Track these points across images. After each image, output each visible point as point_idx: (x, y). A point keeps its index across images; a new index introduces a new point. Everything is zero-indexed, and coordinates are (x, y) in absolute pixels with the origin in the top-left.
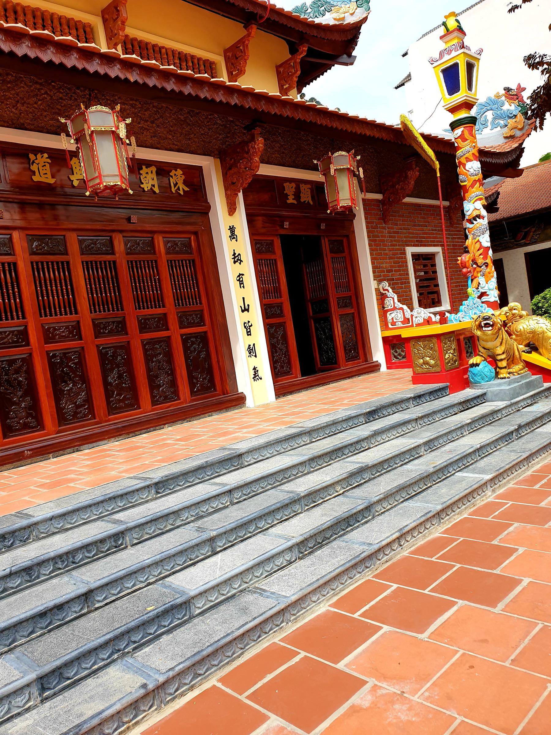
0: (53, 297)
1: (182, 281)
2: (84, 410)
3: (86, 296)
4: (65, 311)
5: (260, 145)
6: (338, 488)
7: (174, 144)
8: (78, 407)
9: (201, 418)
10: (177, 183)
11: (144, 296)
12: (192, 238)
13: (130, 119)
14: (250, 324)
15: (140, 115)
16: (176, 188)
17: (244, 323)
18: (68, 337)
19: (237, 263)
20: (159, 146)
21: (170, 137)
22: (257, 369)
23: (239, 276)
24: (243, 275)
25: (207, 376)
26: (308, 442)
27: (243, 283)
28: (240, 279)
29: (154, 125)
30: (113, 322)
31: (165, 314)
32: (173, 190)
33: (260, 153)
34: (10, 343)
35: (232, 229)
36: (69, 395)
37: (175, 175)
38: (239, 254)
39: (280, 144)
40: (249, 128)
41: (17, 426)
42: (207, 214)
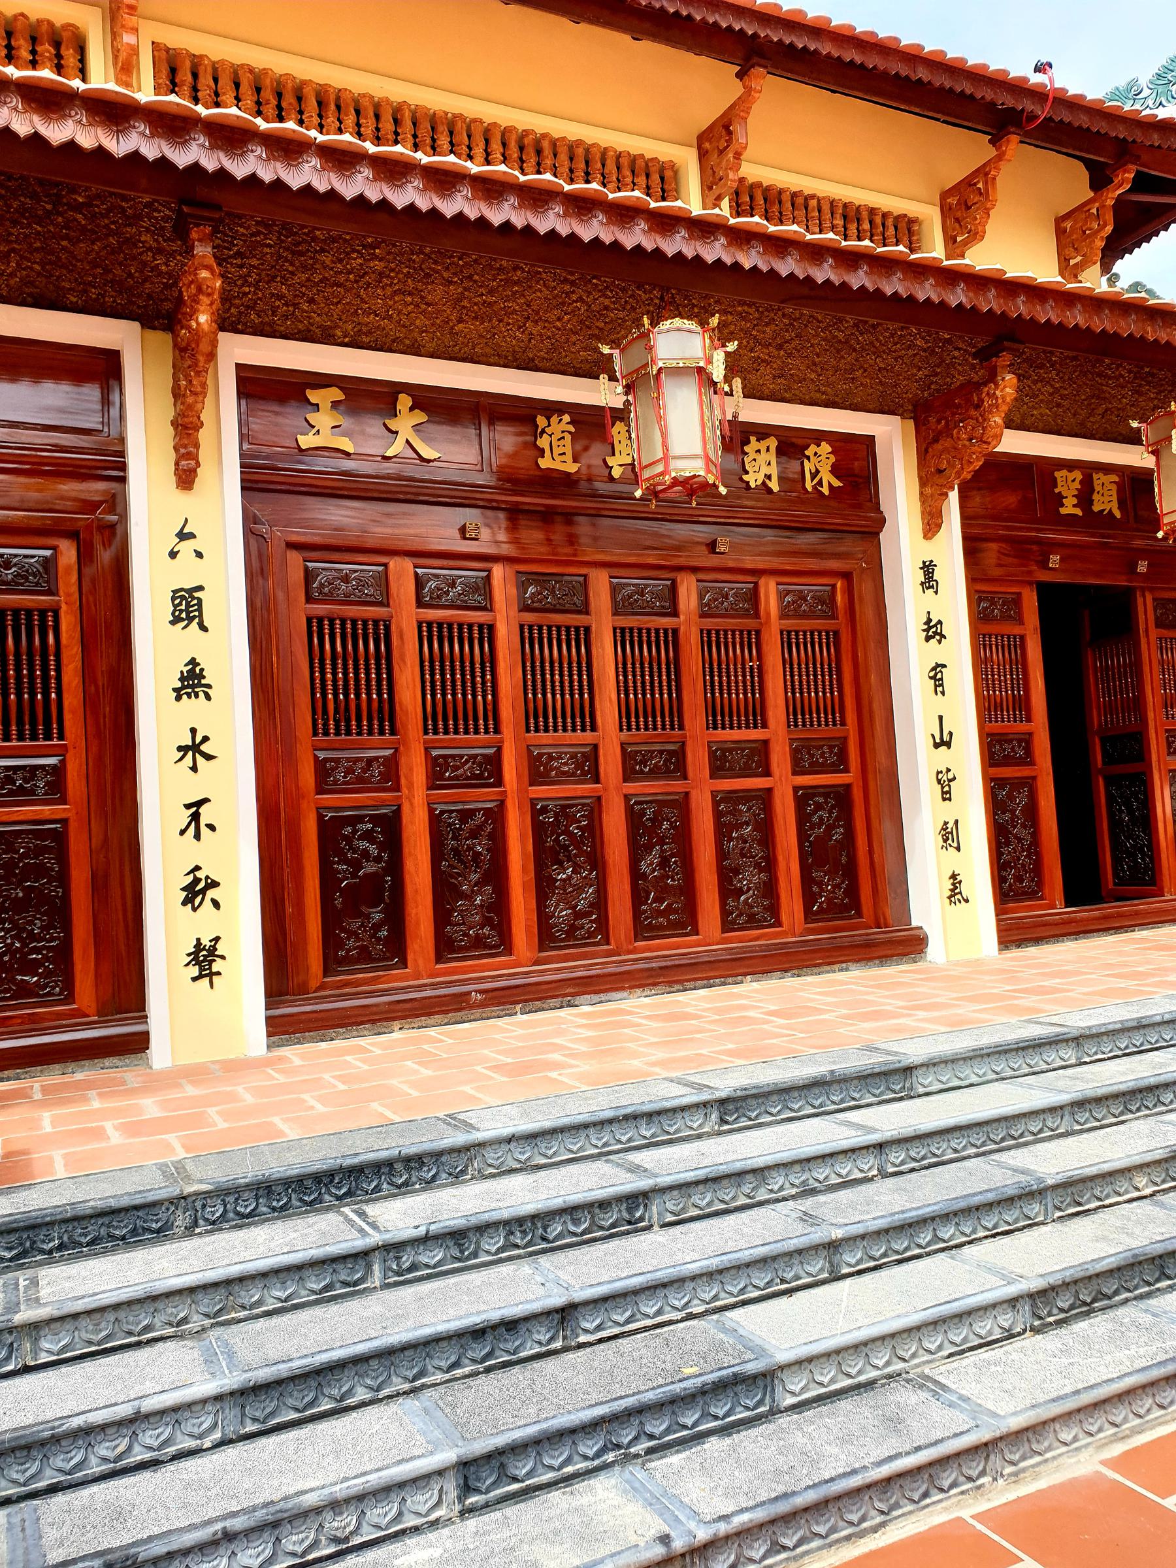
0: (554, 695)
1: (808, 676)
2: (588, 924)
3: (614, 697)
5: (1008, 390)
6: (1141, 1181)
7: (819, 391)
8: (578, 915)
9: (822, 972)
10: (818, 472)
11: (726, 702)
12: (839, 585)
13: (736, 343)
14: (950, 776)
15: (754, 333)
16: (815, 481)
17: (939, 772)
18: (573, 775)
22: (959, 878)
23: (934, 669)
24: (944, 666)
25: (843, 882)
26: (1073, 1061)
27: (942, 685)
28: (936, 674)
29: (782, 353)
30: (661, 752)
31: (766, 743)
32: (809, 486)
33: (1005, 408)
34: (468, 778)
35: (928, 568)
36: (565, 890)
37: (816, 454)
38: (940, 622)
39: (1052, 386)
40: (986, 355)
41: (462, 940)
42: (878, 534)
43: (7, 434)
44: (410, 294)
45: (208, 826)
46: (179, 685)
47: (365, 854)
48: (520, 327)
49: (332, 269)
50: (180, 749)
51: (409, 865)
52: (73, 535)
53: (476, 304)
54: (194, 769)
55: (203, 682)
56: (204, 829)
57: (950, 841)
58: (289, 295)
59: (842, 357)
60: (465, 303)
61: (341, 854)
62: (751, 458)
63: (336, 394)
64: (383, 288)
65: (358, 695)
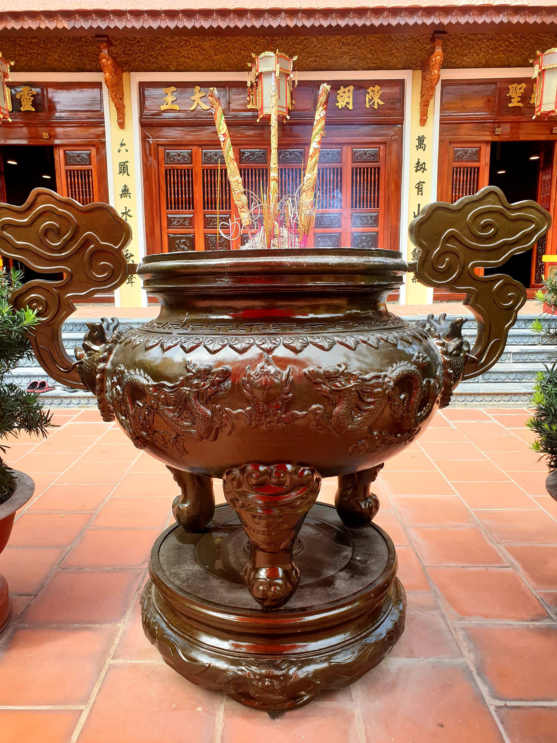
4: (226, 206)
5: (438, 57)
7: (373, 63)
12: (381, 148)
13: (297, 56)
15: (342, 40)
19: (420, 172)
20: (356, 67)
21: (370, 56)
23: (419, 184)
27: (422, 191)
29: (355, 47)
32: (368, 107)
35: (421, 140)
38: (424, 163)
43: (70, 115)
46: (121, 193)
48: (239, 54)
49: (169, 42)
52: (94, 145)
53: (222, 47)
55: (128, 192)
59: (387, 45)
60: (218, 47)
62: (340, 96)
63: (173, 89)
64: (187, 46)
65: (182, 196)
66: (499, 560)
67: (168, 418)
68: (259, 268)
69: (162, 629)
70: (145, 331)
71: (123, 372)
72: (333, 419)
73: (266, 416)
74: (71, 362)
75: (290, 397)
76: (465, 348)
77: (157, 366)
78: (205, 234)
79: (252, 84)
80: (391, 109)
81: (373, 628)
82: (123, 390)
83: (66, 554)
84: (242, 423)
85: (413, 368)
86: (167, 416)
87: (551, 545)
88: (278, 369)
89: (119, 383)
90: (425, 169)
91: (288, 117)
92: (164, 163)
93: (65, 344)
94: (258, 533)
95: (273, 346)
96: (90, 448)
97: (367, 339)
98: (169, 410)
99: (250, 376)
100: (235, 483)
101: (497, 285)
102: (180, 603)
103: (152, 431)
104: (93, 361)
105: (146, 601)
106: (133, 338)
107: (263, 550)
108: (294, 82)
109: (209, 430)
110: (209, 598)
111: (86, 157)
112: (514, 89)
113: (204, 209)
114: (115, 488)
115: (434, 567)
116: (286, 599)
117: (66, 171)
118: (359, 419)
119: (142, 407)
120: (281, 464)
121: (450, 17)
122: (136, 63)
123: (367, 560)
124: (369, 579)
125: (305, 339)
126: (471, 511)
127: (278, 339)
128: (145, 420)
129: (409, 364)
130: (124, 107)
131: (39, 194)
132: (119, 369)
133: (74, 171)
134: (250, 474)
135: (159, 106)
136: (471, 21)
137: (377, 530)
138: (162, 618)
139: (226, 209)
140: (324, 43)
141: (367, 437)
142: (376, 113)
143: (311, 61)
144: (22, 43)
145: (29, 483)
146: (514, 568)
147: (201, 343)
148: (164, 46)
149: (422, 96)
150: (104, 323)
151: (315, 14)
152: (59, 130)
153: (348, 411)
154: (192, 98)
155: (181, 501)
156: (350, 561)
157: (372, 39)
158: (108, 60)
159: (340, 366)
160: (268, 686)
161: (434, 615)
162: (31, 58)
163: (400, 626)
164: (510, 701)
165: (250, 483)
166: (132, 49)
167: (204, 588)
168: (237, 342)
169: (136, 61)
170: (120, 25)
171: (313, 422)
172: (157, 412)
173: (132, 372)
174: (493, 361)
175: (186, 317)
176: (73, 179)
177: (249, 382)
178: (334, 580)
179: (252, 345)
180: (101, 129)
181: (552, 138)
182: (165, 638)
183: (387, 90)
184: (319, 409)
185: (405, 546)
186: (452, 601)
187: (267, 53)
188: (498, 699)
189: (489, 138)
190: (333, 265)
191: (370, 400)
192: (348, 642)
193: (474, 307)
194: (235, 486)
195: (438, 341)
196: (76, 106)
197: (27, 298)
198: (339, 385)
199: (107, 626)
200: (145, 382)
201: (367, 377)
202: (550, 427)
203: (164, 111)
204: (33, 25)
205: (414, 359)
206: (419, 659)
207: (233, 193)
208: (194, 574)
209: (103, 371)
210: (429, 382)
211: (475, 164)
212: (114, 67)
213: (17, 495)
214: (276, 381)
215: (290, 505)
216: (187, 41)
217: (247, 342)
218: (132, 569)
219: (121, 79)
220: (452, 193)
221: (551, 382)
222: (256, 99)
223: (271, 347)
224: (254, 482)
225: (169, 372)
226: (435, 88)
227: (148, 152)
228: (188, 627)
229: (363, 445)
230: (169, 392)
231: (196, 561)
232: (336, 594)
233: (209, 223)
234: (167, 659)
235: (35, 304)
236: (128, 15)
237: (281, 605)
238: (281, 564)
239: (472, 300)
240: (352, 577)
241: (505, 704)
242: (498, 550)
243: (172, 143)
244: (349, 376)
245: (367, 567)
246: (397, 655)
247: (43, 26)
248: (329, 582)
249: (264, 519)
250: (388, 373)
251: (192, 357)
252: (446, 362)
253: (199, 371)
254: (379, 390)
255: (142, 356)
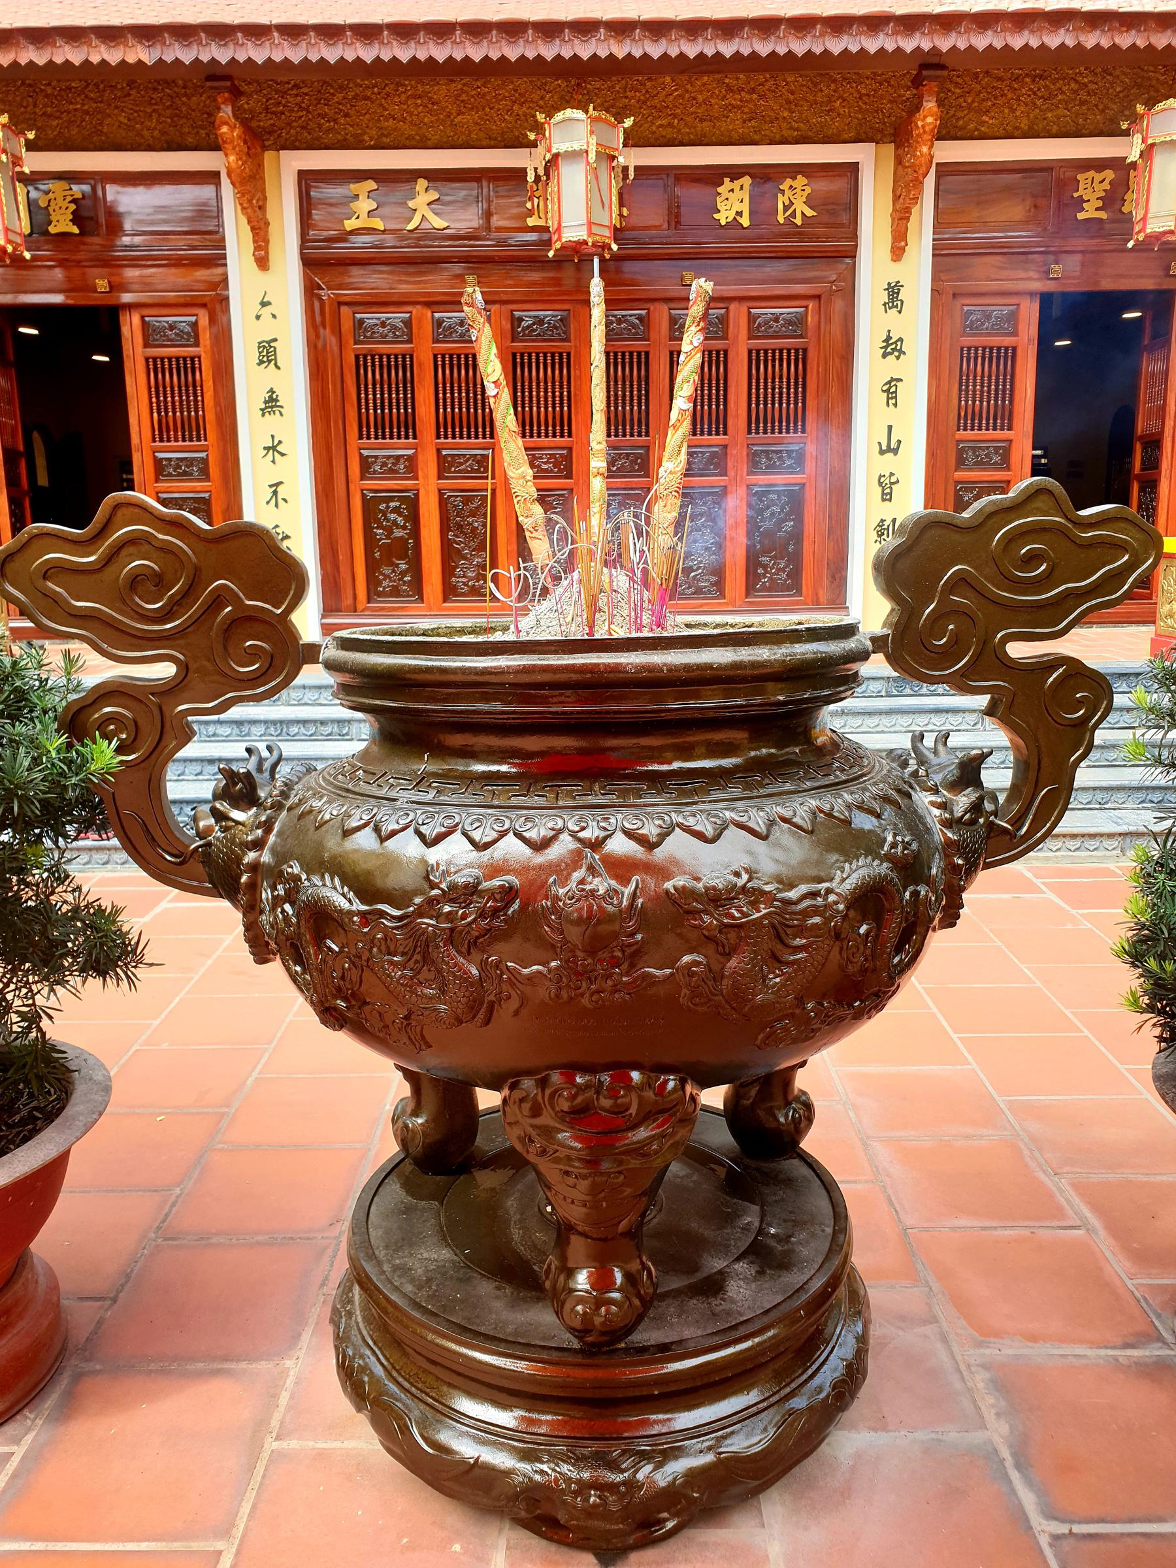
0: (539, 408)
5: (930, 120)
7: (791, 128)
12: (810, 307)
14: (893, 479)
15: (727, 81)
17: (881, 476)
18: (551, 471)
19: (891, 358)
20: (757, 137)
21: (786, 114)
23: (889, 383)
25: (787, 566)
29: (755, 96)
32: (782, 221)
35: (894, 291)
38: (901, 340)
39: (1077, 82)
40: (917, 82)
44: (420, 97)
45: (284, 500)
46: (263, 406)
47: (395, 522)
50: (265, 448)
51: (424, 533)
52: (204, 305)
54: (273, 462)
56: (281, 502)
57: (885, 537)
58: (331, 114)
59: (822, 91)
60: (464, 97)
61: (378, 521)
62: (723, 198)
63: (371, 185)
64: (399, 96)
66: (1058, 1213)
67: (391, 978)
68: (575, 677)
69: (379, 1381)
70: (341, 788)
71: (297, 879)
72: (725, 982)
73: (590, 979)
74: (187, 842)
75: (637, 942)
76: (988, 806)
77: (369, 873)
78: (439, 490)
79: (537, 179)
80: (827, 225)
81: (805, 1377)
82: (298, 917)
83: (173, 1205)
84: (544, 992)
85: (884, 868)
86: (389, 976)
87: (1164, 1178)
88: (613, 883)
89: (290, 897)
90: (901, 352)
91: (615, 247)
92: (352, 342)
93: (175, 810)
94: (573, 1202)
95: (603, 834)
96: (210, 962)
97: (791, 813)
98: (392, 963)
99: (557, 898)
100: (526, 1106)
101: (1054, 676)
102: (414, 1332)
103: (357, 999)
104: (233, 842)
105: (343, 1320)
106: (317, 804)
107: (584, 1235)
108: (625, 169)
109: (473, 1006)
110: (473, 1323)
111: (188, 329)
112: (1089, 181)
113: (438, 437)
114: (267, 1055)
115: (926, 1229)
116: (630, 1329)
117: (147, 359)
118: (778, 980)
119: (338, 954)
120: (620, 1068)
121: (954, 34)
122: (292, 131)
123: (790, 1233)
124: (795, 1278)
125: (667, 818)
126: (1000, 1101)
127: (613, 820)
128: (343, 978)
129: (876, 862)
130: (267, 224)
131: (117, 506)
132: (289, 870)
133: (162, 359)
134: (556, 1091)
135: (341, 221)
136: (998, 44)
137: (810, 1166)
138: (378, 1359)
139: (484, 437)
140: (688, 86)
141: (793, 1015)
142: (800, 234)
143: (661, 126)
144: (49, 91)
145: (98, 1076)
146: (1088, 1230)
147: (457, 825)
148: (351, 95)
149: (896, 198)
150: (253, 758)
151: (670, 30)
152: (131, 273)
153: (754, 966)
154: (411, 204)
155: (409, 1110)
156: (755, 1238)
157: (789, 79)
158: (232, 128)
159: (737, 874)
160: (595, 1506)
161: (926, 1336)
162: (70, 122)
163: (857, 1369)
164: (1079, 1523)
165: (557, 1109)
166: (284, 101)
167: (462, 1301)
168: (530, 825)
169: (292, 127)
170: (259, 54)
171: (685, 991)
172: (368, 966)
173: (316, 880)
174: (1044, 830)
175: (425, 765)
176: (160, 376)
177: (555, 910)
178: (724, 1280)
179: (560, 831)
180: (219, 270)
181: (1168, 285)
182: (384, 1402)
183: (824, 186)
184: (697, 964)
185: (866, 1182)
186: (962, 1304)
187: (569, 113)
188: (1056, 1519)
189: (1037, 286)
190: (720, 667)
191: (798, 942)
192: (754, 1409)
193: (1007, 722)
194: (526, 1112)
195: (933, 798)
196: (165, 222)
197: (96, 716)
198: (737, 914)
199: (263, 1365)
200: (345, 905)
201: (793, 894)
202: (1161, 966)
203: (352, 232)
204: (74, 55)
205: (886, 848)
206: (896, 1434)
207: (515, 501)
208: (441, 1270)
209: (255, 867)
210: (916, 894)
211: (1007, 341)
212: (245, 142)
213: (77, 1107)
214: (610, 908)
215: (639, 1150)
216: (399, 84)
217: (550, 825)
218: (308, 1239)
219: (260, 165)
220: (960, 401)
221: (1162, 866)
222: (546, 206)
223: (597, 837)
224: (565, 1106)
225: (395, 880)
226: (922, 183)
227: (318, 318)
228: (430, 1380)
229: (786, 1029)
230: (394, 928)
231: (444, 1239)
232: (729, 1313)
233: (450, 467)
234: (391, 1446)
235: (112, 727)
236: (276, 34)
237: (620, 1340)
238: (621, 1261)
239: (1001, 709)
240: (761, 1273)
241: (1070, 1530)
242: (1054, 1189)
243: (368, 299)
244: (756, 896)
245: (793, 1251)
246: (853, 1426)
247: (95, 59)
248: (713, 1286)
249: (585, 1177)
250: (834, 885)
251: (435, 855)
252: (949, 843)
253: (453, 887)
254: (817, 920)
255: (332, 844)
